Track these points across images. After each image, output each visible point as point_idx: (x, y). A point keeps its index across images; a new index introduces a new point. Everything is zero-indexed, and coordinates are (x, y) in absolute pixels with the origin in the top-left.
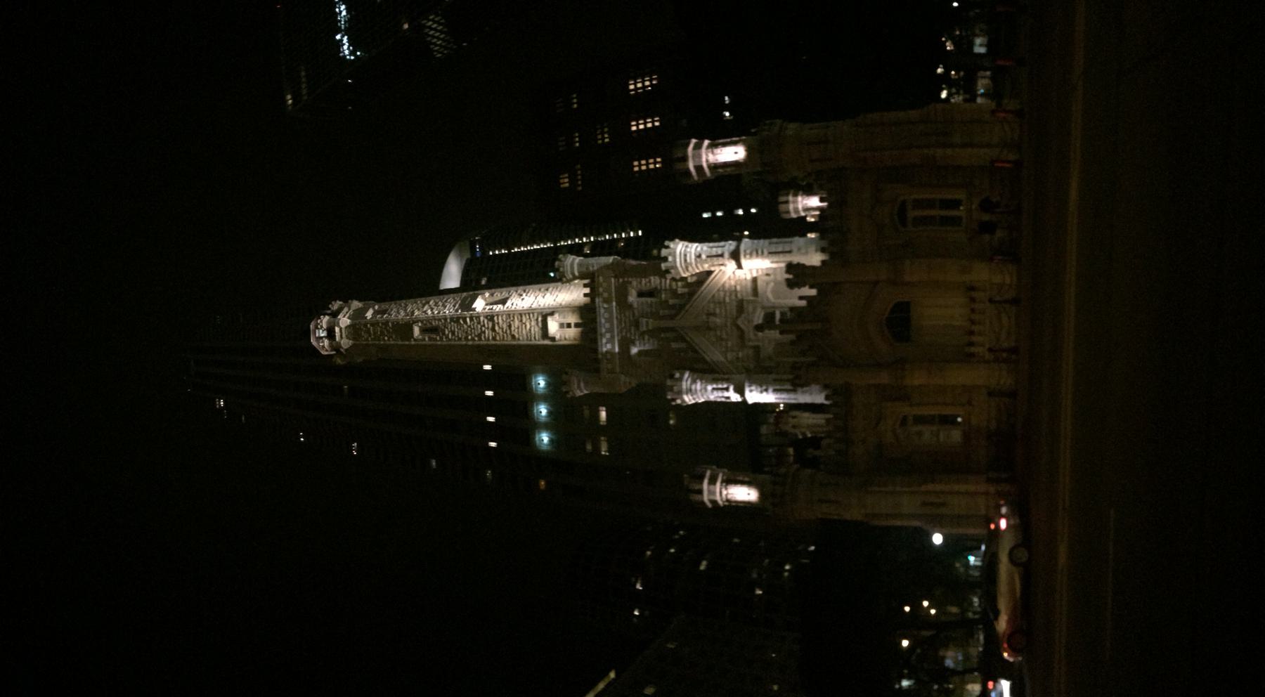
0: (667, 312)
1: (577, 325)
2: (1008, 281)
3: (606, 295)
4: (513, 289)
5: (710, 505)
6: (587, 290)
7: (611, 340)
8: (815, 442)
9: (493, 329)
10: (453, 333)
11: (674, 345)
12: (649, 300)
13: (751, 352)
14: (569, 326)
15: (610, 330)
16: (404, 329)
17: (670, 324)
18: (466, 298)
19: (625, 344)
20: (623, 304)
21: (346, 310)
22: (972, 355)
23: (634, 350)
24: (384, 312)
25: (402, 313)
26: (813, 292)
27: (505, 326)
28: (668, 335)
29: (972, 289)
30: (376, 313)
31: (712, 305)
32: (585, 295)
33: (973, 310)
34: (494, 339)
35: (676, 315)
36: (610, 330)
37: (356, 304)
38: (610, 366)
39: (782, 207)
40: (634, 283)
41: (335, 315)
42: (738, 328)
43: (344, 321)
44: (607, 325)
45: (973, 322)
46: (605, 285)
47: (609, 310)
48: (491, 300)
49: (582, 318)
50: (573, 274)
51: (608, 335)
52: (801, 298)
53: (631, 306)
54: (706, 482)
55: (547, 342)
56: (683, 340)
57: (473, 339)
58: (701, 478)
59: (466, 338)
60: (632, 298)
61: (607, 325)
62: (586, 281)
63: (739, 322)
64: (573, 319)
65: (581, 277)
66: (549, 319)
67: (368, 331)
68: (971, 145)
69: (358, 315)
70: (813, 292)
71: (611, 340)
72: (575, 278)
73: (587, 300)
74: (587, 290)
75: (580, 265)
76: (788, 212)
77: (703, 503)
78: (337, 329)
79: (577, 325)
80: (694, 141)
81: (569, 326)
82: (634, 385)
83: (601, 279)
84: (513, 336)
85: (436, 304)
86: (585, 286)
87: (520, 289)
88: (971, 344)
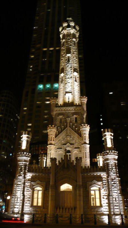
1: (69, 101)
2: (77, 220)
3: (76, 109)
4: (79, 83)
5: (21, 136)
6: (78, 104)
8: (38, 163)
9: (68, 78)
10: (68, 66)
12: (74, 120)
14: (69, 99)
16: (68, 51)
17: (68, 126)
18: (77, 70)
21: (76, 31)
22: (57, 209)
24: (74, 44)
25: (74, 50)
26: (75, 164)
27: (69, 82)
29: (75, 209)
30: (74, 42)
31: (73, 137)
32: (76, 104)
33: (72, 209)
35: (70, 128)
37: (77, 35)
39: (100, 154)
40: (79, 117)
41: (74, 27)
43: (72, 31)
45: (66, 209)
46: (79, 109)
47: (72, 110)
48: (76, 77)
49: (71, 103)
50: (82, 101)
52: (73, 161)
54: (28, 136)
57: (66, 72)
58: (28, 134)
59: (66, 70)
60: (75, 116)
62: (80, 104)
63: (68, 144)
64: (70, 101)
65: (81, 103)
66: (71, 94)
67: (69, 40)
69: (74, 36)
70: (75, 164)
72: (81, 101)
73: (75, 104)
74: (78, 104)
75: (84, 103)
76: (98, 156)
77: (22, 135)
78: (70, 29)
79: (69, 101)
80: (113, 134)
81: (69, 99)
82: (53, 116)
84: (66, 84)
85: (76, 61)
86: (79, 104)
87: (79, 85)
88: (60, 209)
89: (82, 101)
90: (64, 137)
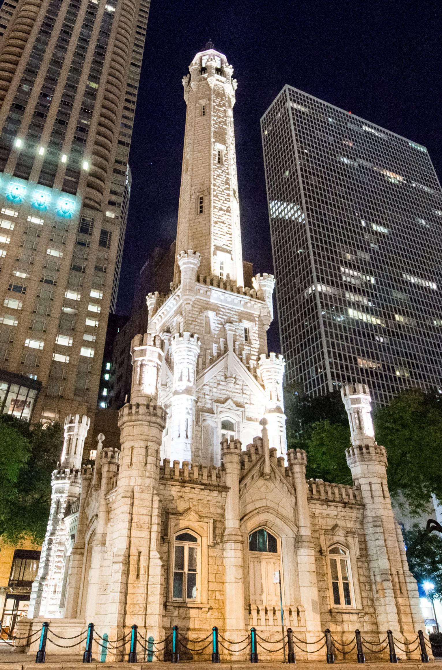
0: (237, 347)
7: (219, 298)
11: (215, 347)
13: (209, 406)
14: (222, 268)
15: (225, 300)
19: (216, 309)
20: (243, 316)
23: (211, 315)
28: (222, 344)
34: (215, 207)
36: (225, 300)
38: (202, 292)
42: (226, 400)
44: (229, 299)
50: (265, 286)
51: (222, 298)
53: (240, 321)
55: (213, 248)
56: (219, 355)
57: (214, 191)
60: (246, 324)
61: (229, 299)
68: (399, 613)
71: (219, 298)
81: (222, 268)
83: (260, 305)
89: (265, 286)
90: (218, 378)
